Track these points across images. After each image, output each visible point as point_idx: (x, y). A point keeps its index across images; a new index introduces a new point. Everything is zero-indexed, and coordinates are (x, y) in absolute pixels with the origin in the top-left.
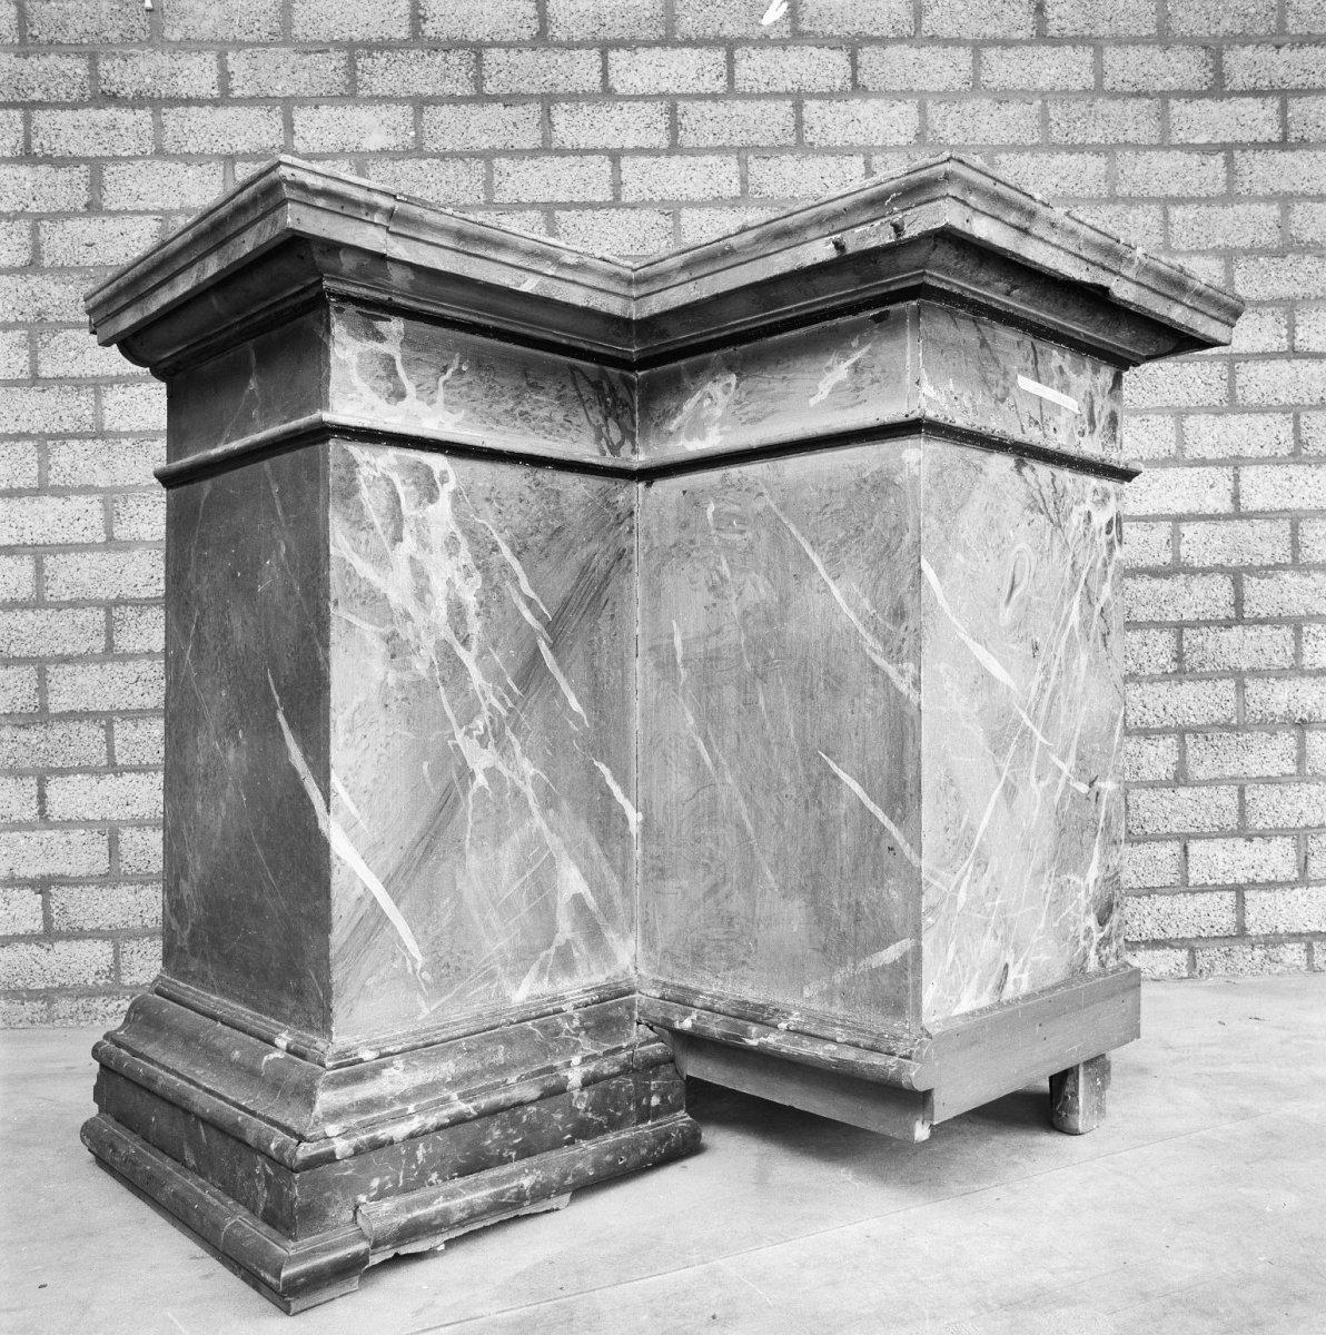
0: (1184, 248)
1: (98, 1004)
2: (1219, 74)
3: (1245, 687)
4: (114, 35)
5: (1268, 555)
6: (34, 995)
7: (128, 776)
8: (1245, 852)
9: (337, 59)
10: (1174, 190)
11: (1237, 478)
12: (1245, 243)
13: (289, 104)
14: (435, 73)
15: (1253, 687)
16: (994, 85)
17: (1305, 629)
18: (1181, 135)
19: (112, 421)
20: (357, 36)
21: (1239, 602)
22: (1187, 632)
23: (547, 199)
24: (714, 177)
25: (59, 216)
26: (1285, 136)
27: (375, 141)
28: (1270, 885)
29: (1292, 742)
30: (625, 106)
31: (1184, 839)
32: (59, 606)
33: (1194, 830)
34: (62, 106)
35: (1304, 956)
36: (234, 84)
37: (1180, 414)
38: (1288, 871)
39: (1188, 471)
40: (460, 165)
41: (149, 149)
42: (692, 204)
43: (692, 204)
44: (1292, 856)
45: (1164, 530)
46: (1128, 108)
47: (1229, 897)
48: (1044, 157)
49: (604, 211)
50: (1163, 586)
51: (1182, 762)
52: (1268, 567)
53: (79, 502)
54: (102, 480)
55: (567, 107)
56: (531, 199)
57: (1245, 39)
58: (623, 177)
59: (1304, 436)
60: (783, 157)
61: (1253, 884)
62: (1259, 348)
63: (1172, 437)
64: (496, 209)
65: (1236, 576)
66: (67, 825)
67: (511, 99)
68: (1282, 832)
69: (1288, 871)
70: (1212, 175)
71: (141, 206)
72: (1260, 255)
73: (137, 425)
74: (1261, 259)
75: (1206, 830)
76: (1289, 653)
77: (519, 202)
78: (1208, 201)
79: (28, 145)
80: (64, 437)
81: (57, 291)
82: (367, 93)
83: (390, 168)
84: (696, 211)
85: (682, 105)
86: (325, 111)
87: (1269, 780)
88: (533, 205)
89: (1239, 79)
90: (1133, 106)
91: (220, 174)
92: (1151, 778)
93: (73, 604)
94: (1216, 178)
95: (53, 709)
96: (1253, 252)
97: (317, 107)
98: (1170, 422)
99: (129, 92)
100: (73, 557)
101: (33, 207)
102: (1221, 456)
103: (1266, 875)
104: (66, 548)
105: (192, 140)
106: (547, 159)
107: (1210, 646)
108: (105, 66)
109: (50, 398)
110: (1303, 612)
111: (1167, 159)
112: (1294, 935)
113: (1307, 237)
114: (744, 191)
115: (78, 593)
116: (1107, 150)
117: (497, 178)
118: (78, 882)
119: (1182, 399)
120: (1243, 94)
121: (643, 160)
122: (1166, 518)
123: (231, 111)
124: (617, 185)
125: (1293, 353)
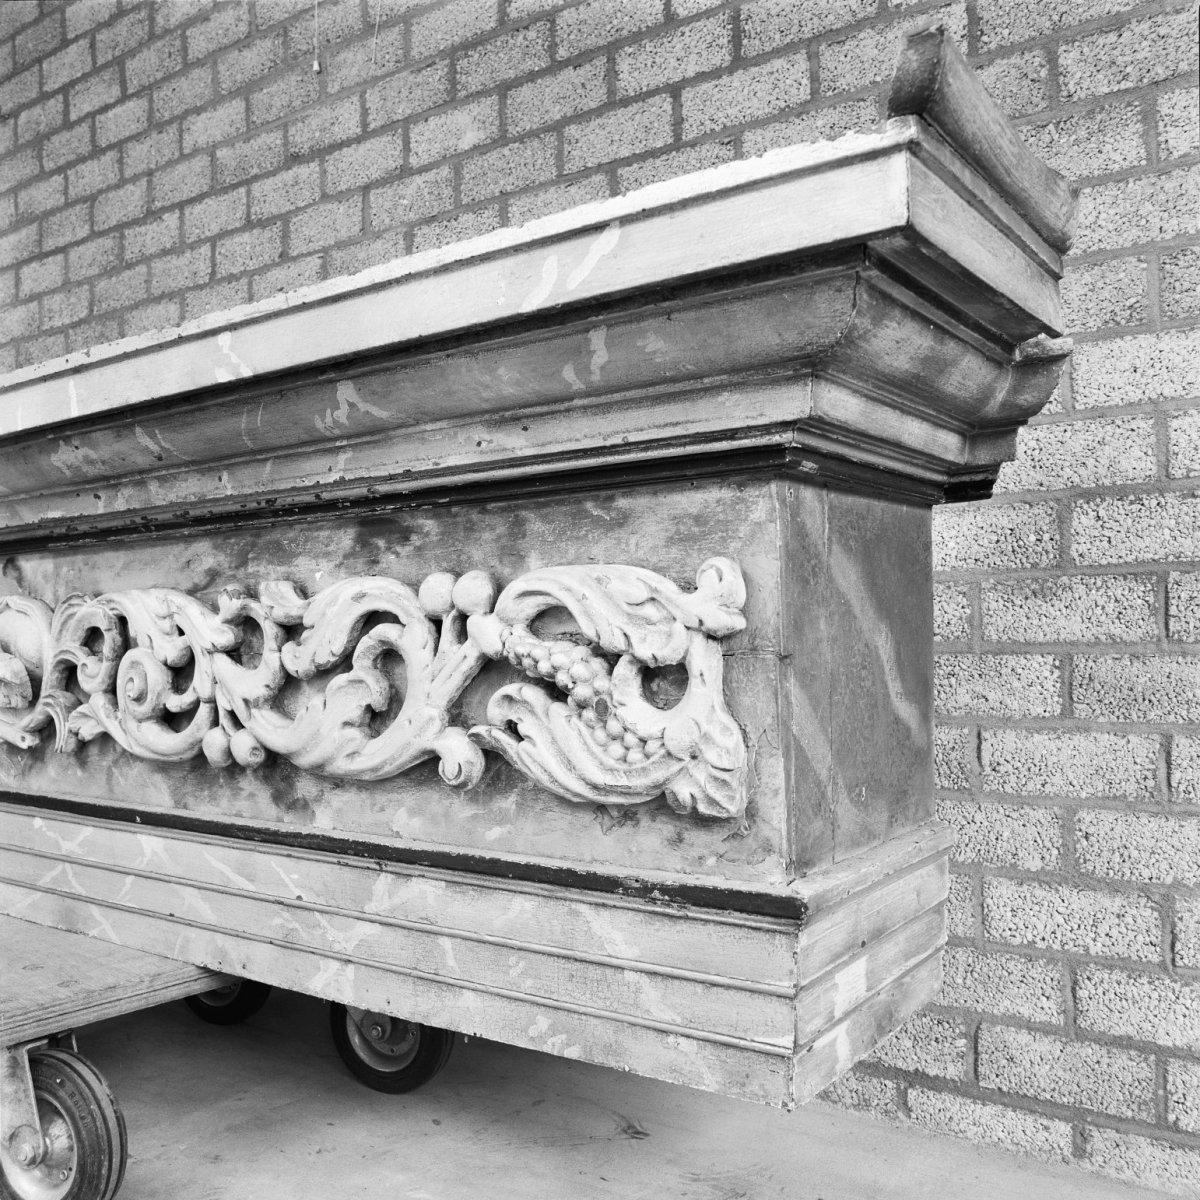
14: (517, 54)
23: (612, 157)
30: (686, 29)
40: (536, 143)
41: (317, 195)
49: (665, 157)
55: (631, 50)
58: (684, 112)
60: (861, 36)
64: (565, 181)
67: (577, 61)
71: (313, 246)
77: (587, 168)
79: (248, 215)
82: (463, 94)
86: (433, 122)
88: (599, 168)
97: (426, 120)
99: (305, 149)
101: (252, 265)
114: (814, 92)
117: (567, 148)
124: (678, 123)
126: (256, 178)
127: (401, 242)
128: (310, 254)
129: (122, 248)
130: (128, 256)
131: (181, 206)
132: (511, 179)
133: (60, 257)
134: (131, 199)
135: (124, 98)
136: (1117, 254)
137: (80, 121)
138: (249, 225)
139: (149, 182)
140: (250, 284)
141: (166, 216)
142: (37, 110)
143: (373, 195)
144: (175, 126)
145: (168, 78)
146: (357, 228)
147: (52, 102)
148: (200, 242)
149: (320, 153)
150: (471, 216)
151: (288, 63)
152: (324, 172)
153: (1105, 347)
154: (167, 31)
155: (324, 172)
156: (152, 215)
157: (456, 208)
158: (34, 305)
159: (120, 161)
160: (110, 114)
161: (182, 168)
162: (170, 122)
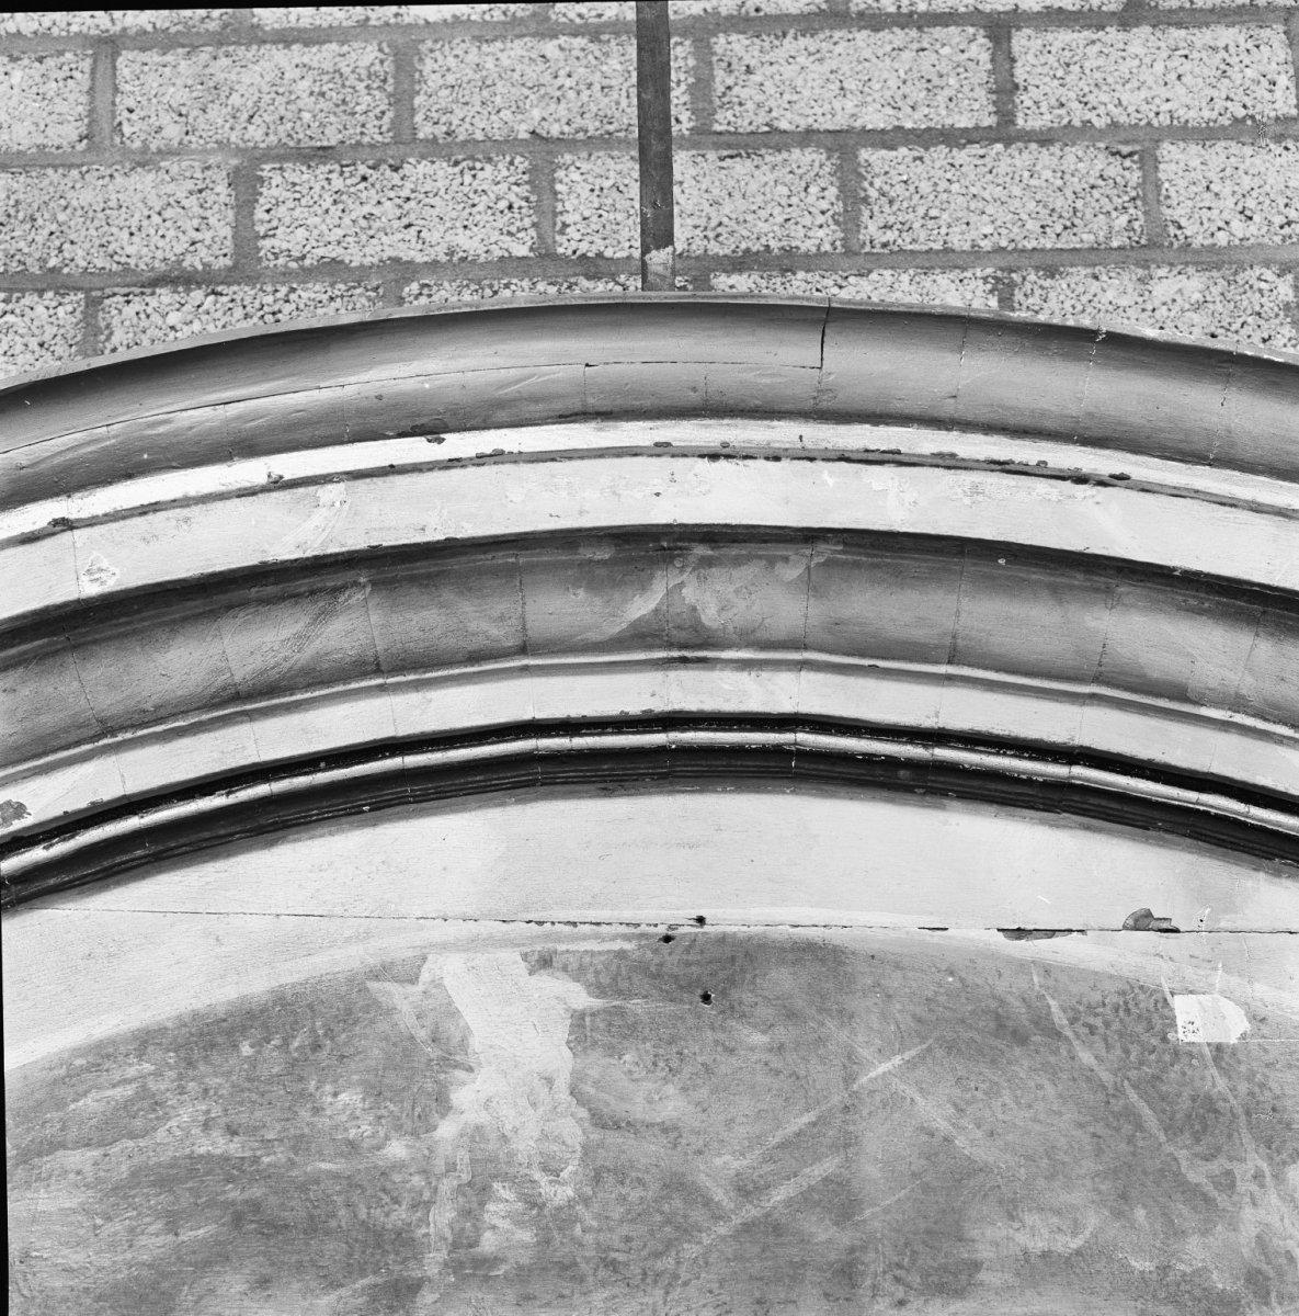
24: (1234, 73)
42: (1183, 132)
43: (1183, 132)
49: (976, 149)
56: (803, 124)
58: (1020, 74)
64: (717, 146)
83: (472, 57)
84: (1194, 149)
88: (807, 137)
91: (83, 79)
106: (837, 34)
121: (1063, 37)
124: (1005, 91)
127: (222, 188)
132: (562, 111)
146: (71, 132)
150: (442, 169)
157: (397, 141)
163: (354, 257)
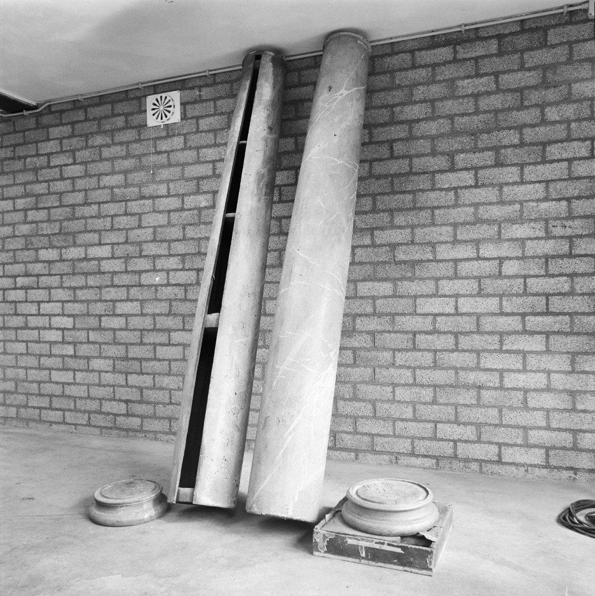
0: (439, 223)
1: (138, 434)
2: (453, 163)
3: (458, 373)
4: (144, 181)
5: (468, 328)
6: (124, 430)
7: (145, 376)
8: (457, 429)
9: (195, 182)
10: (436, 204)
11: (457, 302)
12: (461, 220)
13: (183, 195)
15: (461, 373)
16: (376, 174)
17: (481, 354)
18: (439, 185)
19: (143, 282)
20: (200, 176)
21: (457, 344)
22: (438, 353)
25: (132, 229)
26: (477, 183)
27: (203, 204)
28: (466, 441)
29: (475, 393)
31: (436, 423)
32: (131, 330)
33: (438, 420)
34: (134, 200)
35: (478, 467)
36: (171, 191)
37: (437, 280)
38: (473, 437)
39: (439, 299)
41: (152, 210)
44: (475, 432)
45: (430, 318)
46: (421, 178)
47: (451, 444)
48: (392, 196)
50: (430, 337)
51: (435, 397)
52: (468, 332)
53: (135, 303)
54: (140, 298)
57: (462, 151)
59: (482, 287)
61: (460, 440)
62: (466, 257)
63: (434, 287)
65: (456, 335)
66: (132, 387)
68: (471, 424)
69: (473, 437)
70: (450, 198)
72: (466, 225)
73: (148, 283)
74: (467, 226)
75: (443, 420)
76: (475, 362)
78: (448, 207)
79: (126, 211)
80: (132, 286)
81: (131, 248)
82: (201, 191)
85: (282, 188)
86: (192, 197)
87: (466, 406)
89: (460, 165)
90: (422, 177)
92: (424, 401)
93: (134, 330)
94: (451, 199)
95: (129, 357)
96: (464, 224)
98: (433, 282)
100: (134, 318)
101: (127, 227)
102: (451, 294)
103: (465, 438)
104: (132, 315)
105: (161, 207)
107: (446, 358)
108: (142, 189)
109: (129, 276)
110: (480, 348)
111: (434, 194)
112: (475, 459)
113: (485, 217)
115: (135, 327)
116: (413, 192)
118: (134, 402)
119: (438, 274)
120: (461, 170)
122: (431, 314)
123: (170, 199)
125: (479, 258)
126: (129, 200)
128: (149, 227)
129: (74, 213)
130: (77, 215)
131: (99, 203)
133: (46, 211)
134: (79, 197)
135: (74, 163)
136: (366, 263)
137: (55, 167)
138: (126, 214)
139: (86, 193)
140: (127, 233)
141: (93, 205)
142: (35, 159)
143: (171, 214)
144: (97, 177)
145: (93, 161)
146: (166, 222)
147: (42, 158)
148: (107, 216)
149: (153, 197)
151: (141, 168)
152: (154, 204)
153: (363, 283)
154: (93, 147)
155: (154, 204)
156: (86, 204)
158: (34, 225)
159: (73, 184)
160: (69, 167)
161: (99, 191)
162: (95, 175)
163: (195, 237)
